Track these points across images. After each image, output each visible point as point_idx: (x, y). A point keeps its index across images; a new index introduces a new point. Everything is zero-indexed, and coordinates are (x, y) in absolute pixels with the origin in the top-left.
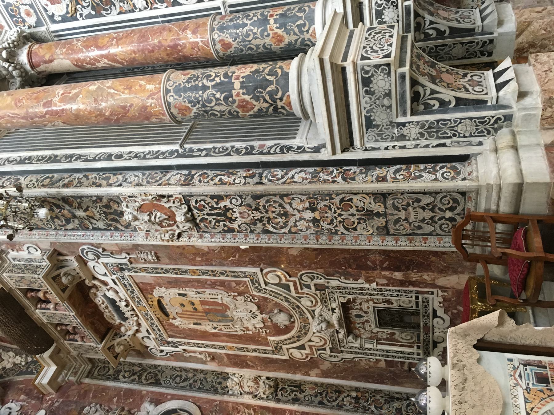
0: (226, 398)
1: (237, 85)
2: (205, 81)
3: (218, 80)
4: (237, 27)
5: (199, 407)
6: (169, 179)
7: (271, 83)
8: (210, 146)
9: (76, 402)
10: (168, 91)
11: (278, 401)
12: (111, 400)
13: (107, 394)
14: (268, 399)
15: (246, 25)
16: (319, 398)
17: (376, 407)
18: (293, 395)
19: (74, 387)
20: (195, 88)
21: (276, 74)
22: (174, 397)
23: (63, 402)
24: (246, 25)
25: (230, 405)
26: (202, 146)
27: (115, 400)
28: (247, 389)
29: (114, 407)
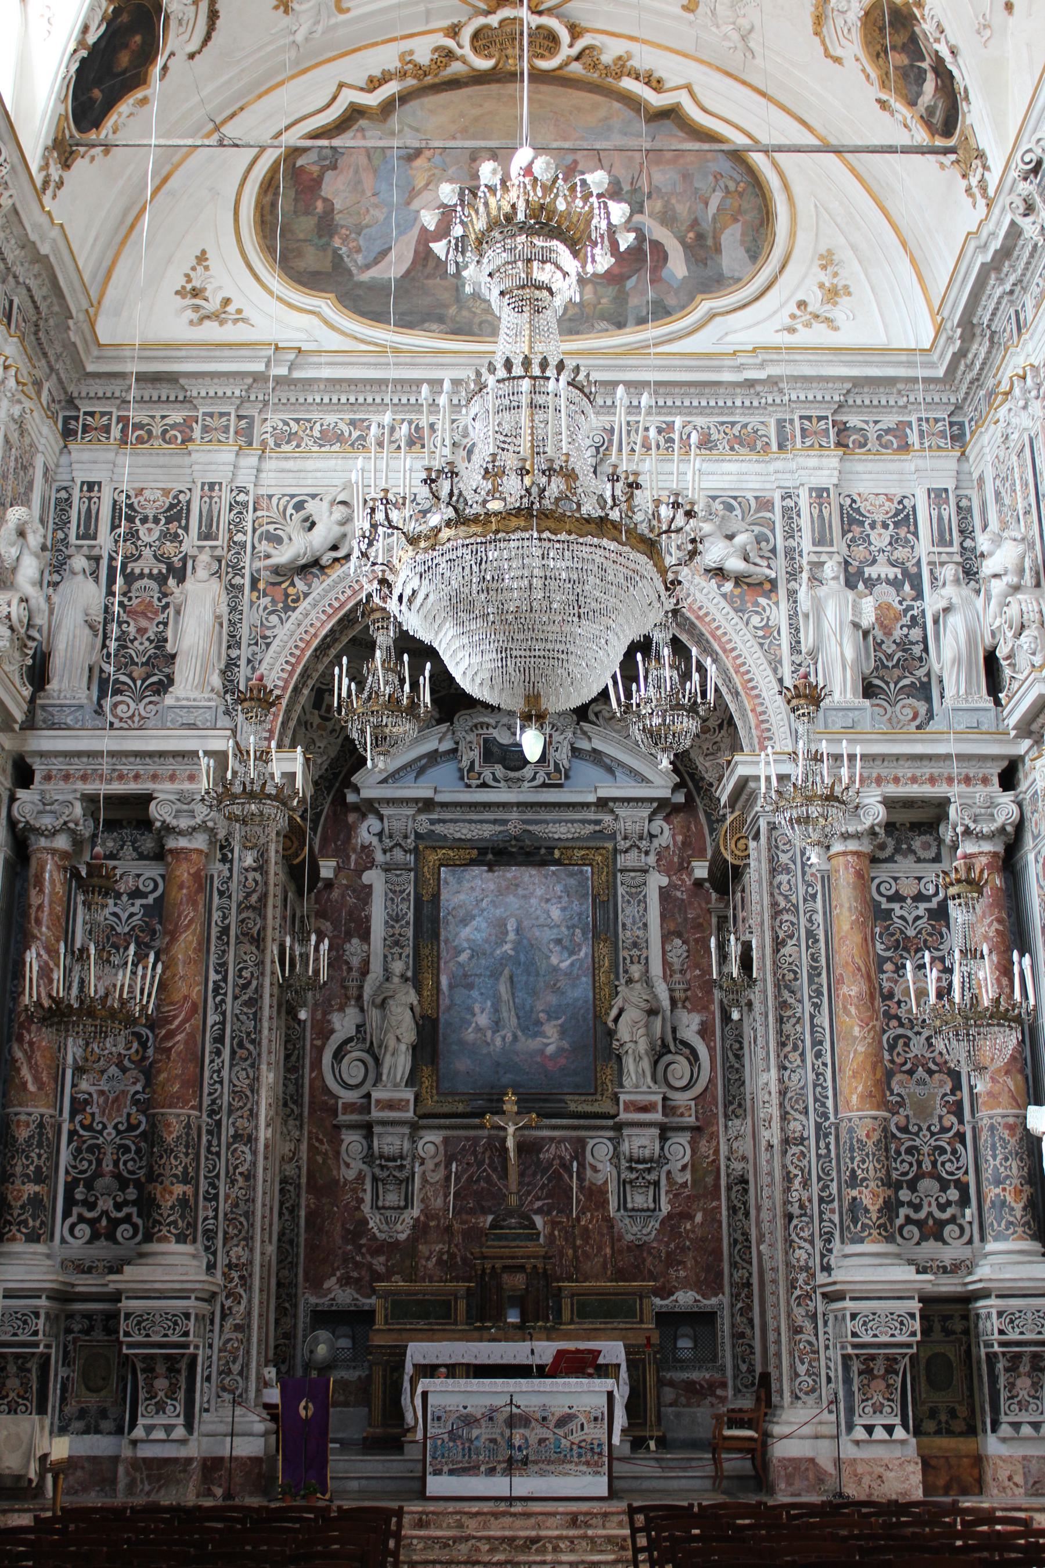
0: (721, 1121)
1: (854, 1193)
2: (858, 1159)
3: (859, 1172)
4: (994, 1148)
5: (707, 1088)
6: (795, 1119)
7: (855, 1227)
8: (833, 1154)
9: (686, 919)
10: (850, 1120)
11: (729, 1188)
12: (697, 966)
13: (703, 957)
14: (728, 1175)
15: (995, 1159)
16: (741, 1238)
17: (741, 1309)
18: (739, 1205)
19: (704, 905)
20: (852, 1149)
21: (863, 1230)
22: (711, 1050)
23: (683, 900)
24: (995, 1159)
25: (715, 1128)
26: (832, 1147)
27: (698, 972)
28: (735, 1146)
29: (688, 976)
